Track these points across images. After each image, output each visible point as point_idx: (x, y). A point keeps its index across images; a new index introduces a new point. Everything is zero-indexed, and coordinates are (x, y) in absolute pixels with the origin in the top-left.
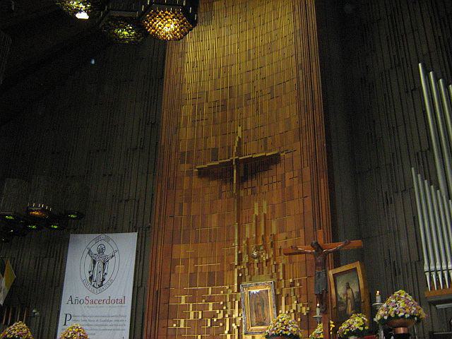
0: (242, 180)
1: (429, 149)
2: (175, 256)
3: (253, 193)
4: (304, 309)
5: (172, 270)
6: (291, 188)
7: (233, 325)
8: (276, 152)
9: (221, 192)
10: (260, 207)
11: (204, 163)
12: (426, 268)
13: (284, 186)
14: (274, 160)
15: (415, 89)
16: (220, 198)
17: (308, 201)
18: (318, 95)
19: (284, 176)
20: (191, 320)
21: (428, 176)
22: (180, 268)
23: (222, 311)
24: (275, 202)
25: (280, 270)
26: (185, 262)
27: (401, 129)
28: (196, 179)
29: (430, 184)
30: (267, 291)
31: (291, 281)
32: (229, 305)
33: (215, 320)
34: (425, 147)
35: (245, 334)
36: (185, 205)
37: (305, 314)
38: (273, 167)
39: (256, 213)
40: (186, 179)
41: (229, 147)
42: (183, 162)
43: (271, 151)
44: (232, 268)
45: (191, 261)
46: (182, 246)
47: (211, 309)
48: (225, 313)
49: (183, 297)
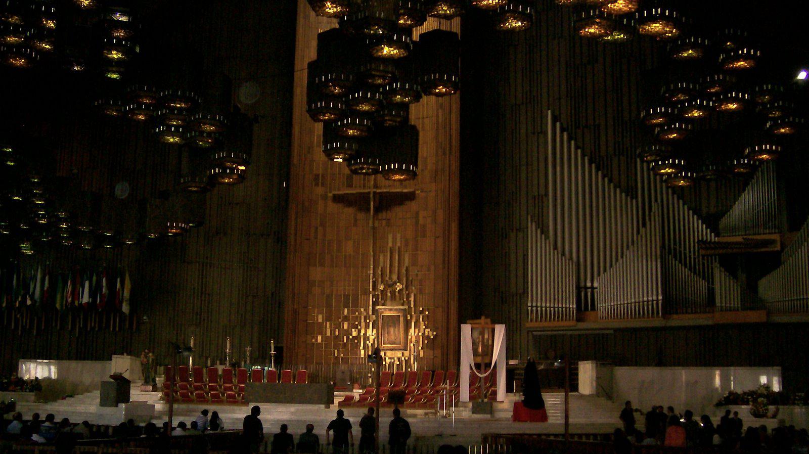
0: (378, 210)
4: (430, 333)
6: (424, 226)
7: (368, 342)
8: (411, 190)
9: (356, 220)
10: (394, 239)
11: (339, 190)
12: (529, 304)
15: (541, 132)
16: (355, 225)
17: (440, 241)
18: (456, 143)
19: (417, 213)
20: (328, 337)
21: (541, 226)
22: (316, 290)
23: (357, 330)
25: (412, 299)
27: (524, 168)
28: (331, 203)
29: (542, 233)
31: (421, 309)
32: (363, 324)
33: (351, 337)
34: (542, 192)
36: (320, 229)
37: (432, 337)
38: (407, 202)
39: (390, 244)
40: (320, 202)
42: (317, 185)
44: (366, 293)
46: (319, 269)
47: (346, 327)
48: (359, 332)
49: (320, 317)
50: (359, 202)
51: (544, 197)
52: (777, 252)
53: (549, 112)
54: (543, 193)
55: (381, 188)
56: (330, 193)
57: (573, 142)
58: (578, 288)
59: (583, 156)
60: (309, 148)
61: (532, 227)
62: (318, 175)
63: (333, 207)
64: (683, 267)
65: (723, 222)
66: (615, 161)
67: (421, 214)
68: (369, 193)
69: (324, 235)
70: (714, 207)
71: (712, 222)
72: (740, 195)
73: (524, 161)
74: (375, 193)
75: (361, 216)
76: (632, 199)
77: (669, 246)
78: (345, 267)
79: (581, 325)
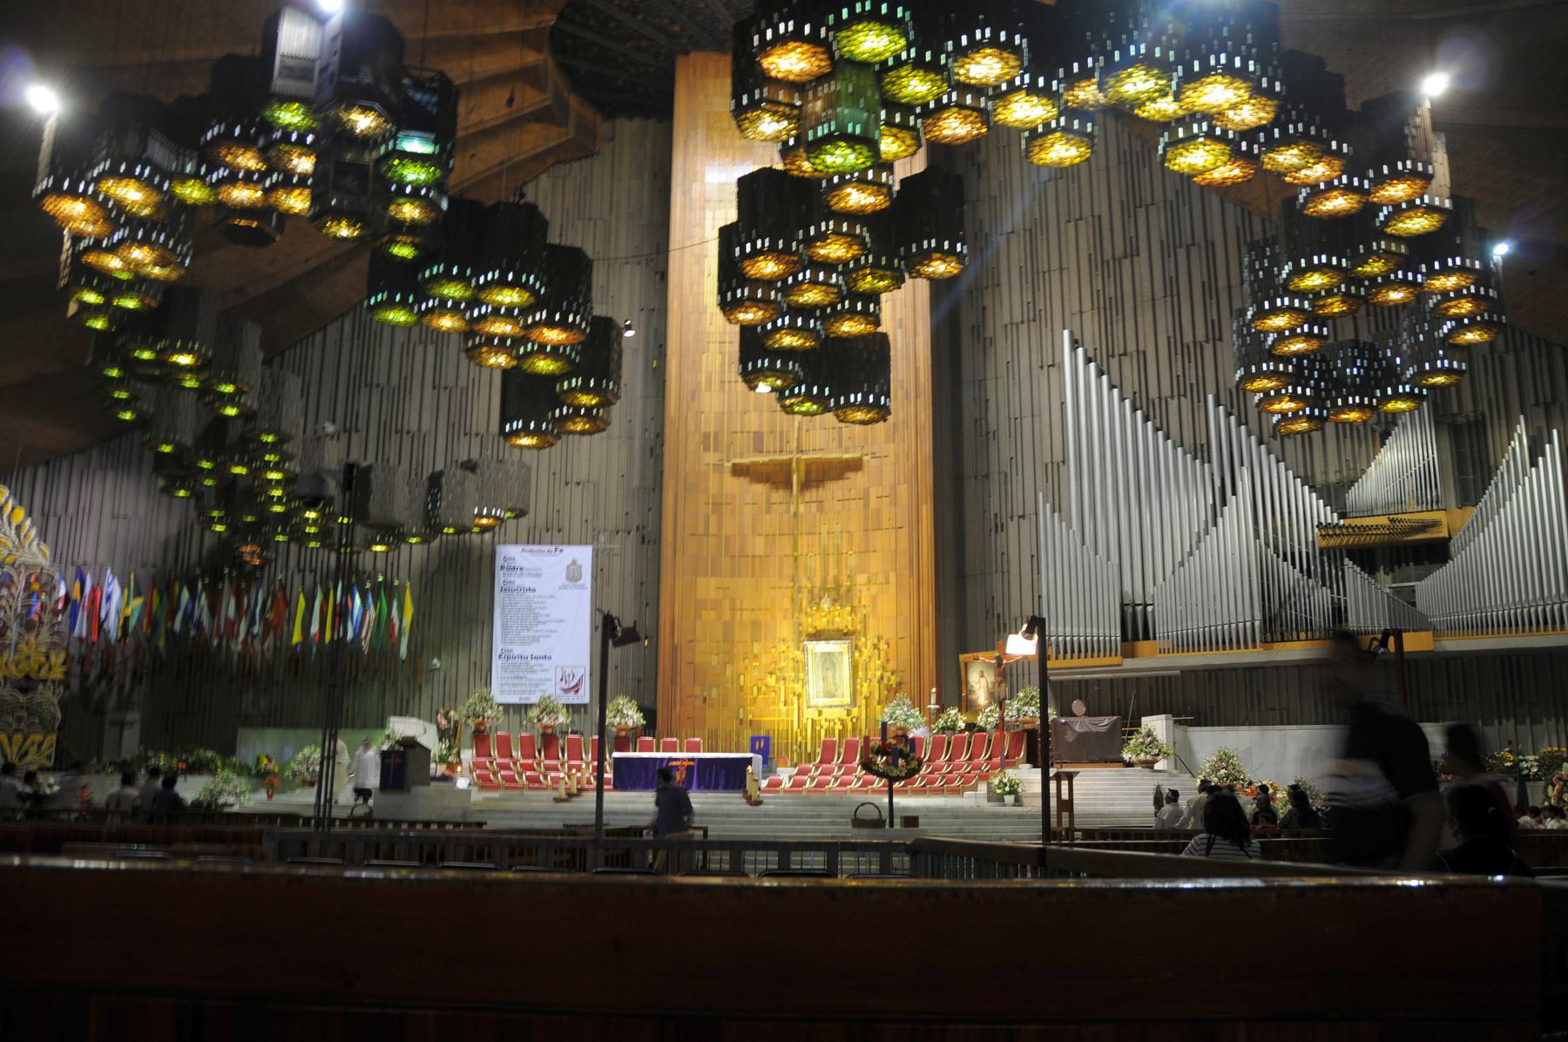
1: (1063, 462)
2: (701, 594)
3: (821, 509)
5: (698, 616)
6: (878, 511)
8: (857, 455)
9: (769, 504)
11: (741, 457)
13: (866, 505)
14: (855, 465)
15: (1053, 365)
16: (768, 511)
17: (904, 533)
19: (867, 491)
22: (708, 615)
24: (853, 528)
26: (716, 606)
30: (841, 653)
35: (808, 707)
36: (713, 519)
38: (849, 475)
41: (781, 433)
42: (707, 449)
43: (847, 451)
45: (727, 604)
50: (776, 476)
51: (1061, 464)
52: (1444, 538)
53: (1066, 333)
54: (1060, 459)
55: (807, 452)
56: (728, 461)
57: (1105, 378)
58: (1123, 606)
59: (1122, 399)
60: (694, 393)
61: (1045, 509)
62: (707, 435)
63: (733, 485)
64: (1291, 567)
65: (1355, 495)
66: (1173, 404)
67: (873, 493)
68: (790, 461)
69: (720, 528)
70: (1336, 472)
71: (1334, 494)
72: (1375, 454)
73: (1027, 411)
74: (798, 460)
75: (779, 495)
76: (1203, 463)
77: (1266, 534)
78: (753, 576)
79: (1129, 663)
